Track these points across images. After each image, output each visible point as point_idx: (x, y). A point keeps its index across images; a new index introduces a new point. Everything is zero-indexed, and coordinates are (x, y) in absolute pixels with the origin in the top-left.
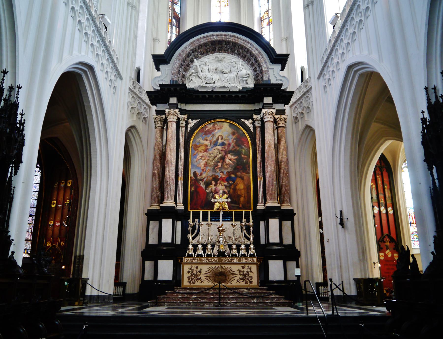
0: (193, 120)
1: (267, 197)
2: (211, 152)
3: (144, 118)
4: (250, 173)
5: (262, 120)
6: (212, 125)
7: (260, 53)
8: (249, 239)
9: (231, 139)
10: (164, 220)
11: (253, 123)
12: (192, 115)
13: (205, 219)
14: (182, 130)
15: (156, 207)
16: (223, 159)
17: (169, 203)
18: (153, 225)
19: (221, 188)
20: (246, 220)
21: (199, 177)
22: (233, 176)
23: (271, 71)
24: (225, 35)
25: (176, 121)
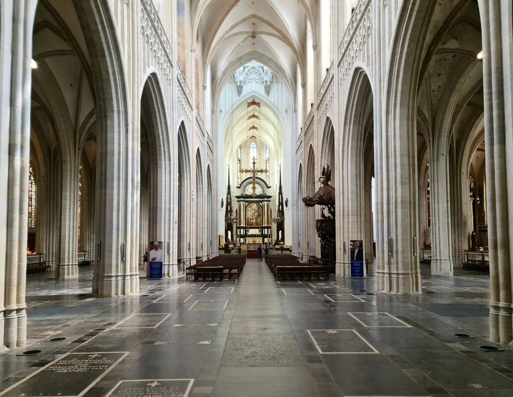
9: (256, 209)
10: (241, 229)
11: (262, 204)
12: (247, 202)
14: (244, 206)
15: (238, 226)
16: (254, 213)
17: (242, 225)
19: (254, 221)
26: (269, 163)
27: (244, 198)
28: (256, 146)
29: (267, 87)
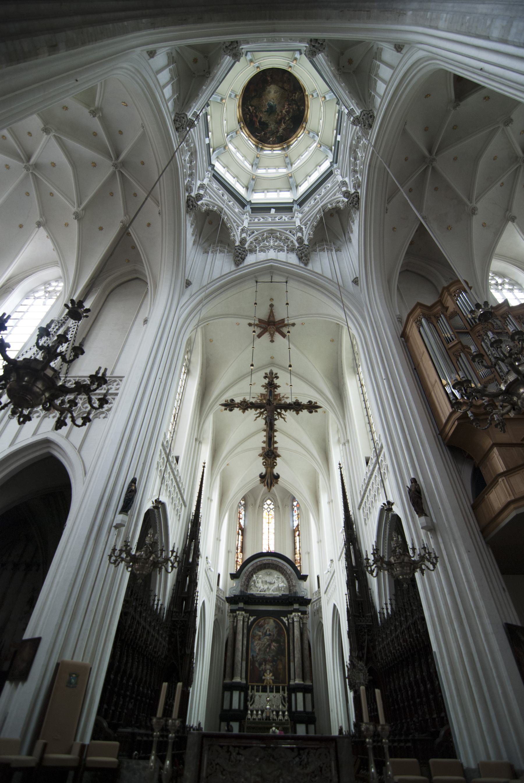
0: (252, 617)
1: (296, 676)
2: (262, 641)
3: (222, 611)
4: (285, 657)
5: (293, 618)
6: (263, 621)
7: (291, 573)
8: (285, 706)
9: (275, 630)
11: (288, 620)
12: (251, 613)
13: (258, 691)
14: (246, 624)
15: (227, 681)
16: (269, 645)
17: (237, 679)
18: (227, 694)
19: (268, 667)
20: (283, 692)
21: (255, 659)
22: (276, 658)
23: (297, 585)
24: (272, 560)
25: (242, 619)
26: (299, 535)
27: (246, 603)
28: (273, 507)
29: (303, 249)
